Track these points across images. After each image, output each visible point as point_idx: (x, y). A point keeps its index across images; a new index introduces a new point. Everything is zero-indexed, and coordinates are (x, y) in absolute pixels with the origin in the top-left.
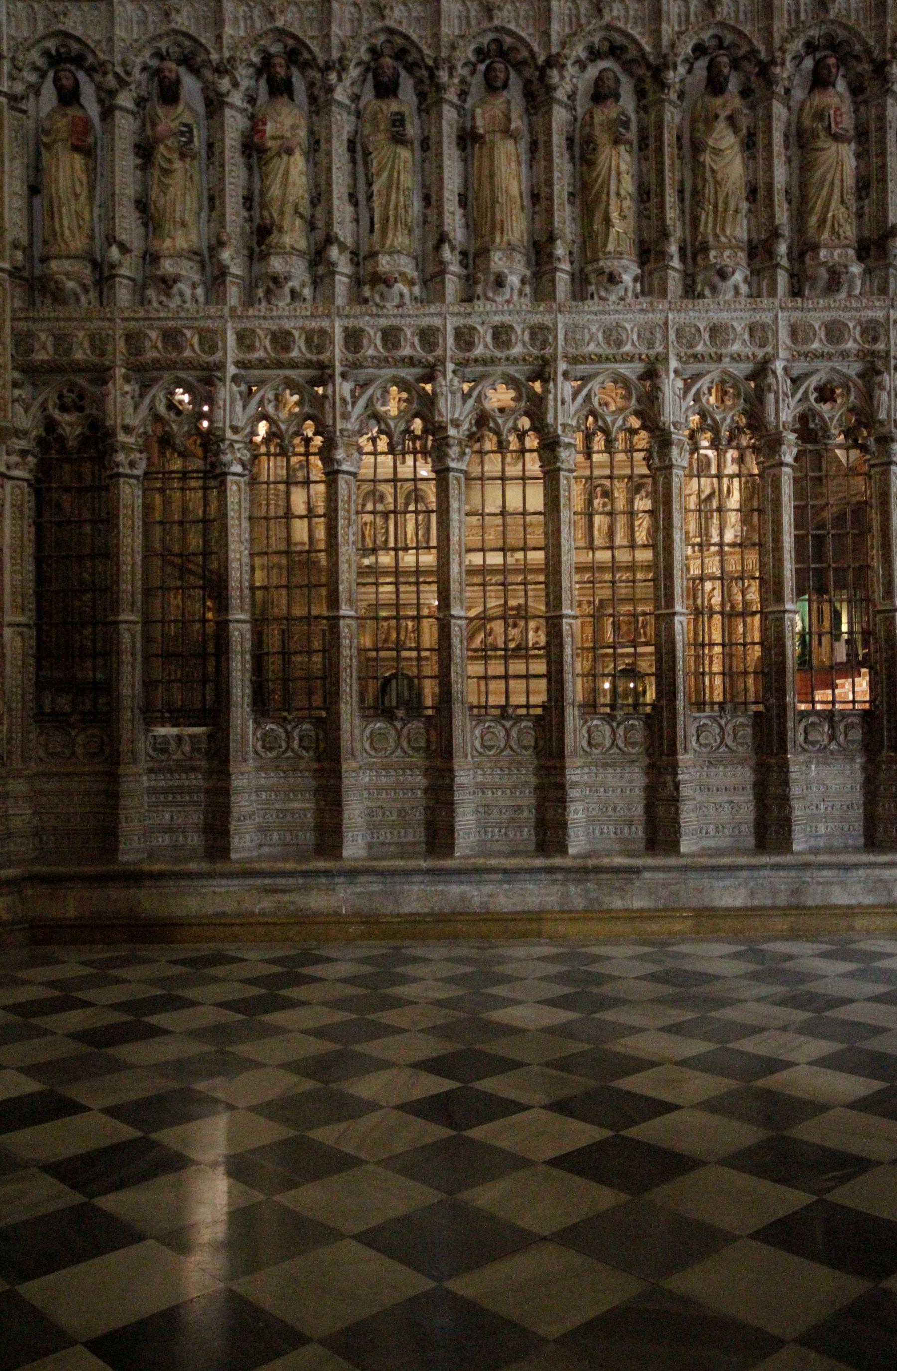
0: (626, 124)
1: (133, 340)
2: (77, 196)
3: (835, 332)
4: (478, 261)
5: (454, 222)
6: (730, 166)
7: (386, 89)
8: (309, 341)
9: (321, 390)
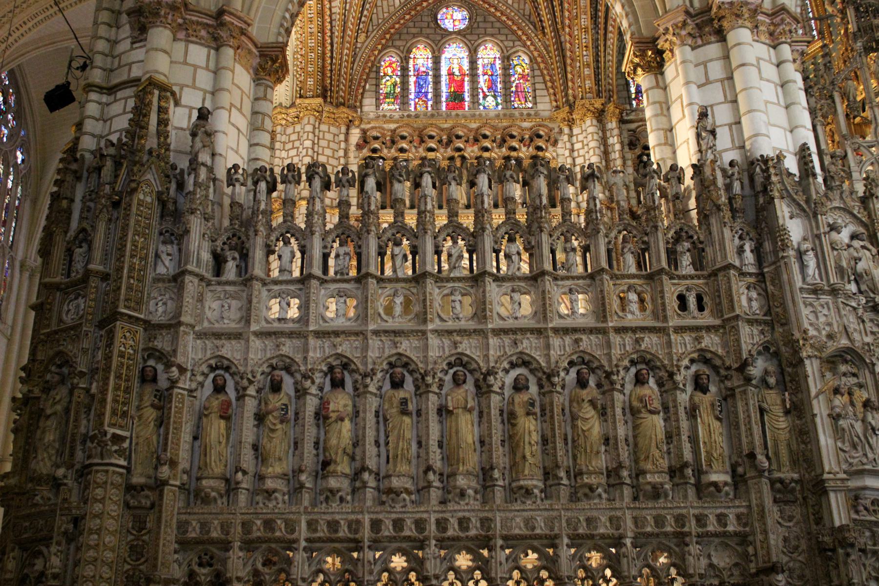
0: (532, 405)
1: (246, 526)
2: (220, 443)
4: (450, 480)
5: (436, 458)
6: (594, 427)
7: (397, 384)
8: (349, 527)
9: (355, 555)
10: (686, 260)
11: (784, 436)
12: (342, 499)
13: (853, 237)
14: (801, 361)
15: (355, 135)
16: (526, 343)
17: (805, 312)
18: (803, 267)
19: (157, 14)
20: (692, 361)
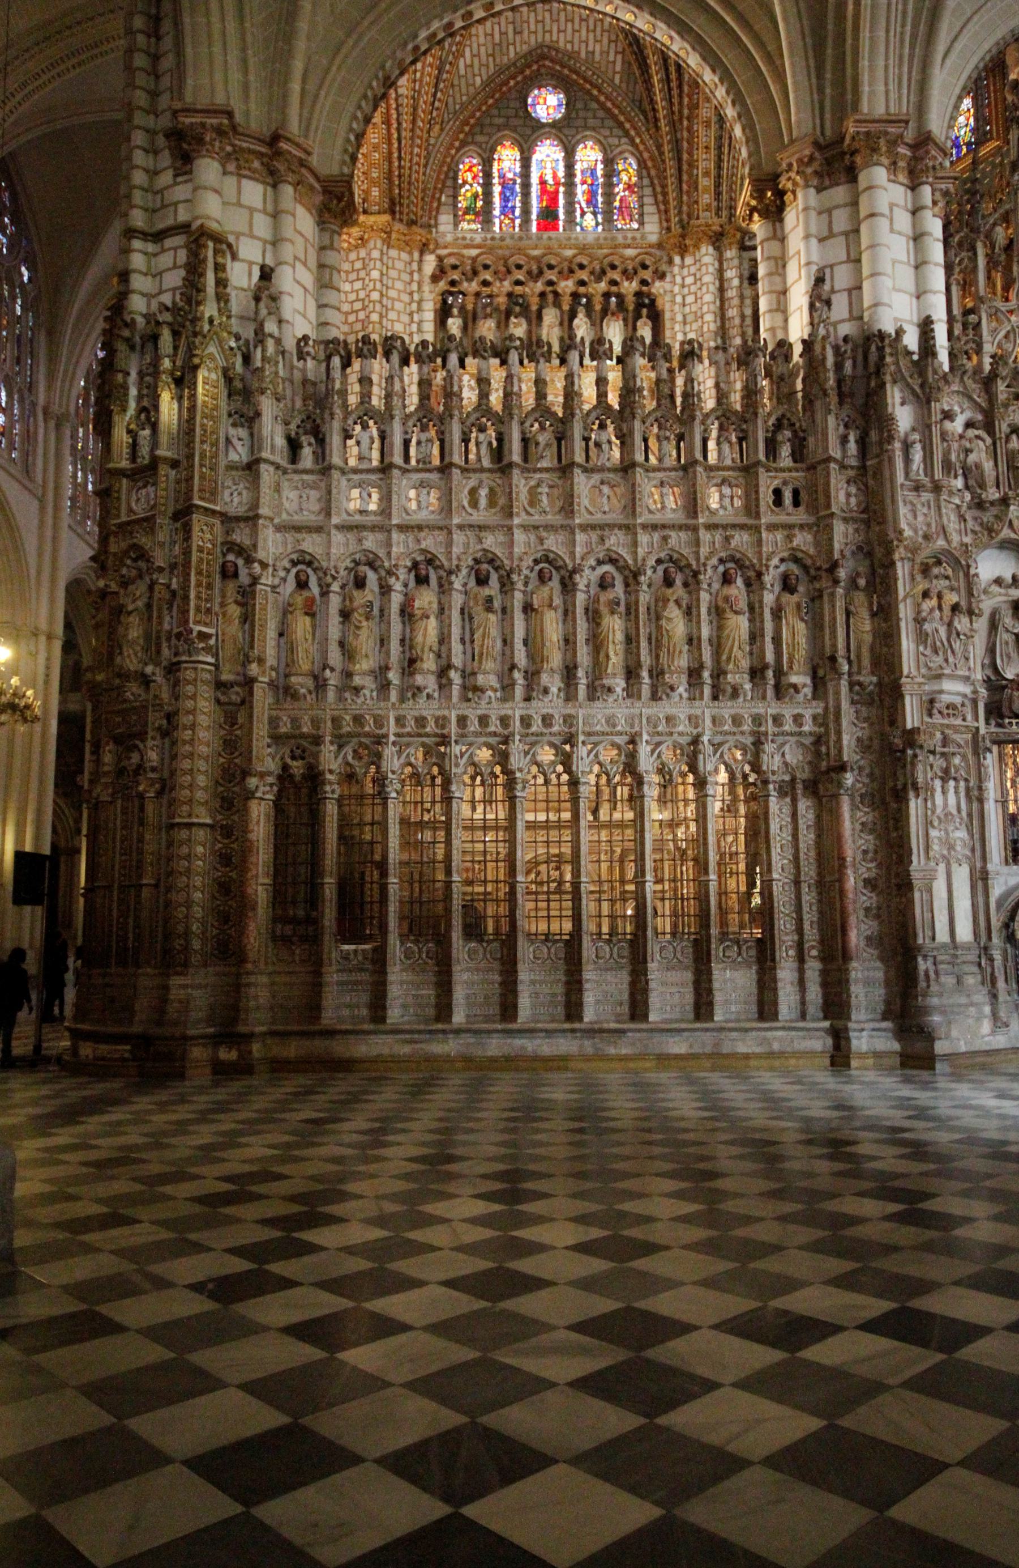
0: (618, 604)
1: (336, 721)
3: (737, 720)
5: (521, 656)
6: (677, 625)
7: (482, 581)
10: (785, 451)
11: (868, 638)
12: (429, 696)
13: (969, 425)
14: (893, 564)
15: (430, 263)
16: (613, 540)
17: (903, 511)
18: (908, 460)
19: (200, 141)
20: (782, 560)
